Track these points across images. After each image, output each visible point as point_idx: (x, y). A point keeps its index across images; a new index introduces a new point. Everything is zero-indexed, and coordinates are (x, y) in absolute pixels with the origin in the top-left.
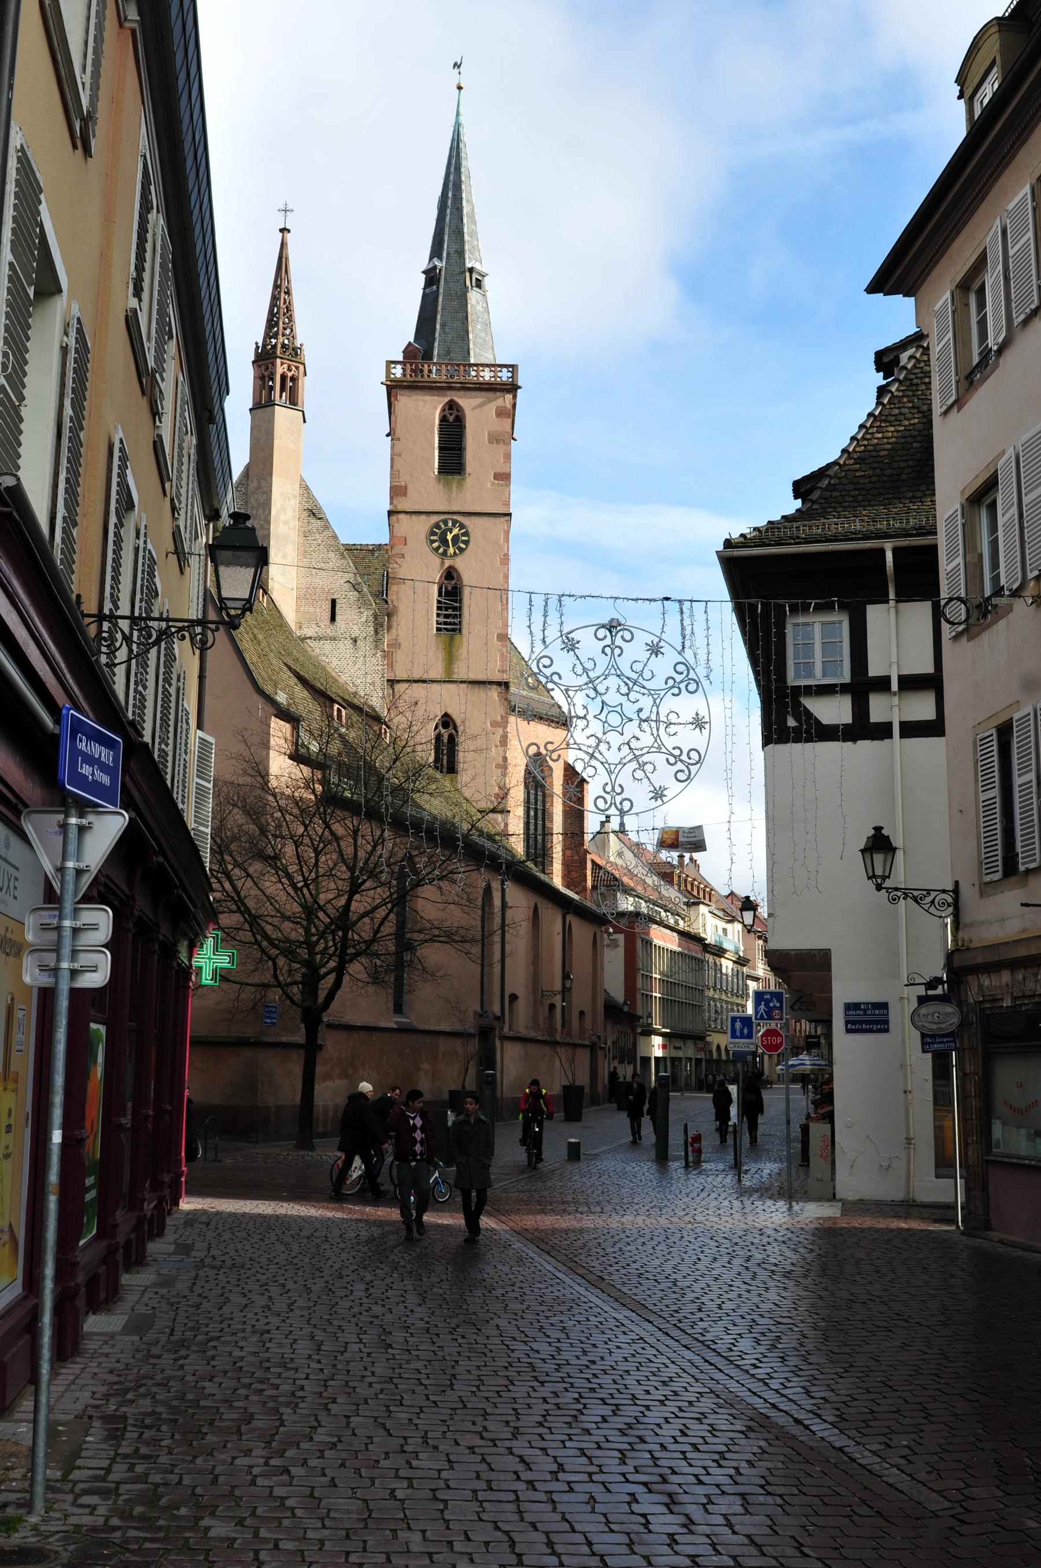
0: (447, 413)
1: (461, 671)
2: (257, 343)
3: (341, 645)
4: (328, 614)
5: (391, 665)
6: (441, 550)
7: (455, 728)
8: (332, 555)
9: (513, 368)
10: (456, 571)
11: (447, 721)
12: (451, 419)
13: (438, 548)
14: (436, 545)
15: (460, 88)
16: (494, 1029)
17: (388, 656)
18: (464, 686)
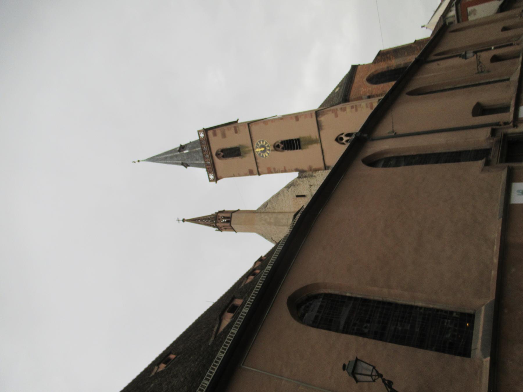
4: (303, 198)
7: (342, 134)
8: (280, 198)
9: (199, 132)
10: (275, 144)
12: (222, 154)
14: (267, 155)
15: (139, 161)
16: (505, 135)
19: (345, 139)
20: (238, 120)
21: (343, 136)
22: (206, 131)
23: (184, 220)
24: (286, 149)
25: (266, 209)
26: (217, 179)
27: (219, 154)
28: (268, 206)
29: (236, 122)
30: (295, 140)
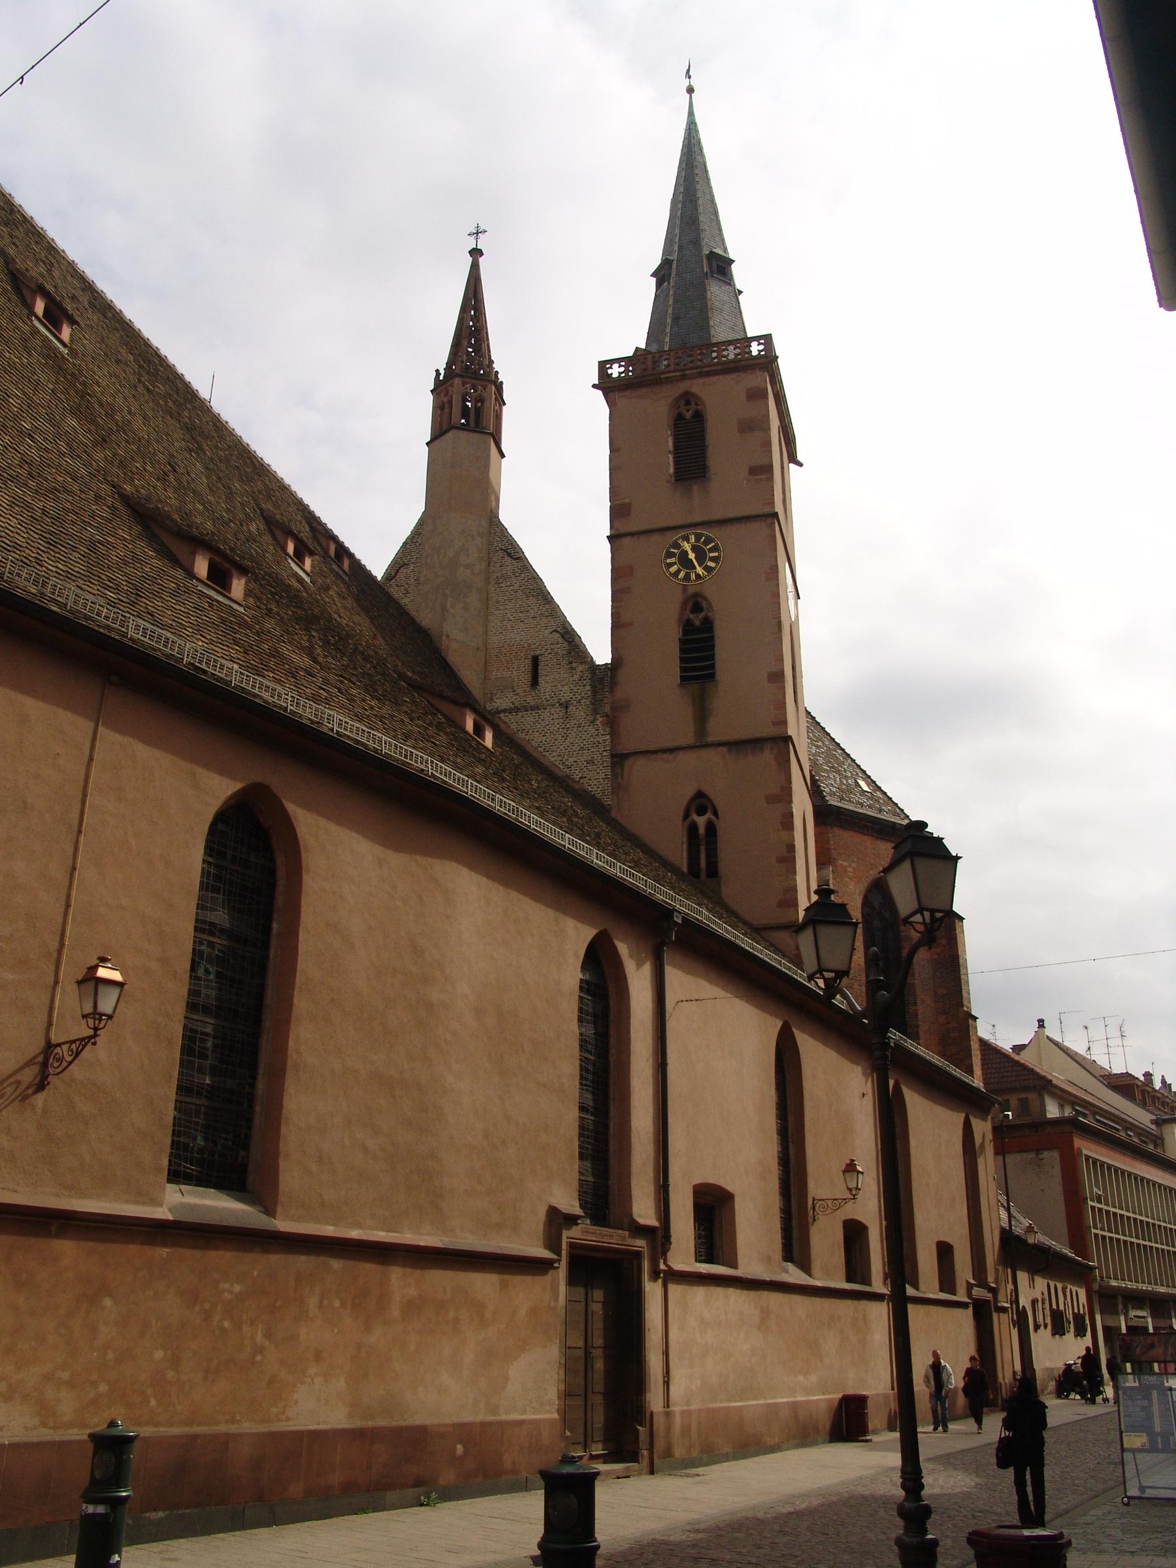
0: (682, 409)
1: (718, 729)
2: (437, 371)
3: (545, 714)
4: (527, 678)
5: (614, 735)
6: (682, 575)
7: (716, 814)
8: (532, 600)
9: (767, 340)
10: (705, 598)
11: (701, 802)
12: (688, 415)
13: (678, 571)
14: (674, 569)
15: (690, 90)
17: (612, 724)
18: (724, 749)
19: (701, 821)
20: (800, 465)
21: (709, 815)
22: (768, 363)
23: (476, 253)
24: (685, 632)
25: (501, 554)
26: (606, 385)
27: (688, 403)
28: (508, 560)
29: (793, 459)
30: (713, 666)
